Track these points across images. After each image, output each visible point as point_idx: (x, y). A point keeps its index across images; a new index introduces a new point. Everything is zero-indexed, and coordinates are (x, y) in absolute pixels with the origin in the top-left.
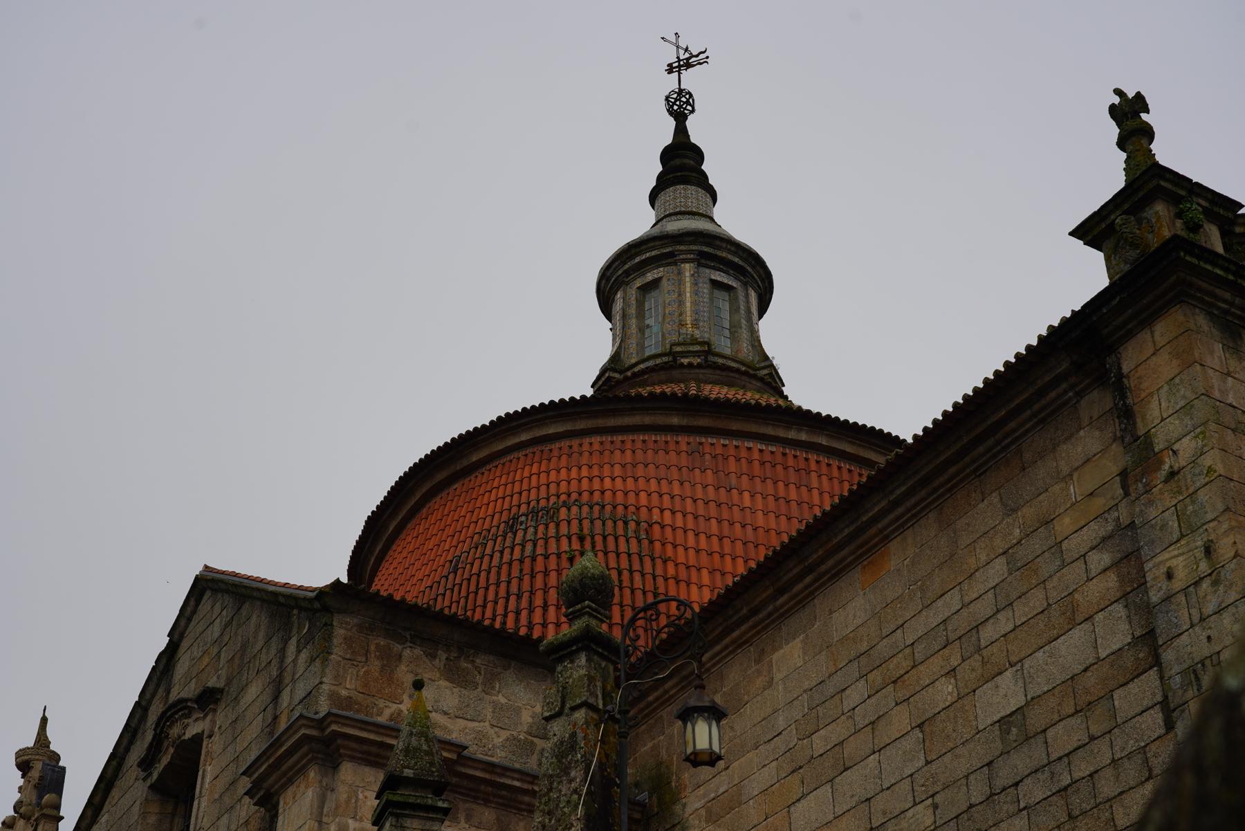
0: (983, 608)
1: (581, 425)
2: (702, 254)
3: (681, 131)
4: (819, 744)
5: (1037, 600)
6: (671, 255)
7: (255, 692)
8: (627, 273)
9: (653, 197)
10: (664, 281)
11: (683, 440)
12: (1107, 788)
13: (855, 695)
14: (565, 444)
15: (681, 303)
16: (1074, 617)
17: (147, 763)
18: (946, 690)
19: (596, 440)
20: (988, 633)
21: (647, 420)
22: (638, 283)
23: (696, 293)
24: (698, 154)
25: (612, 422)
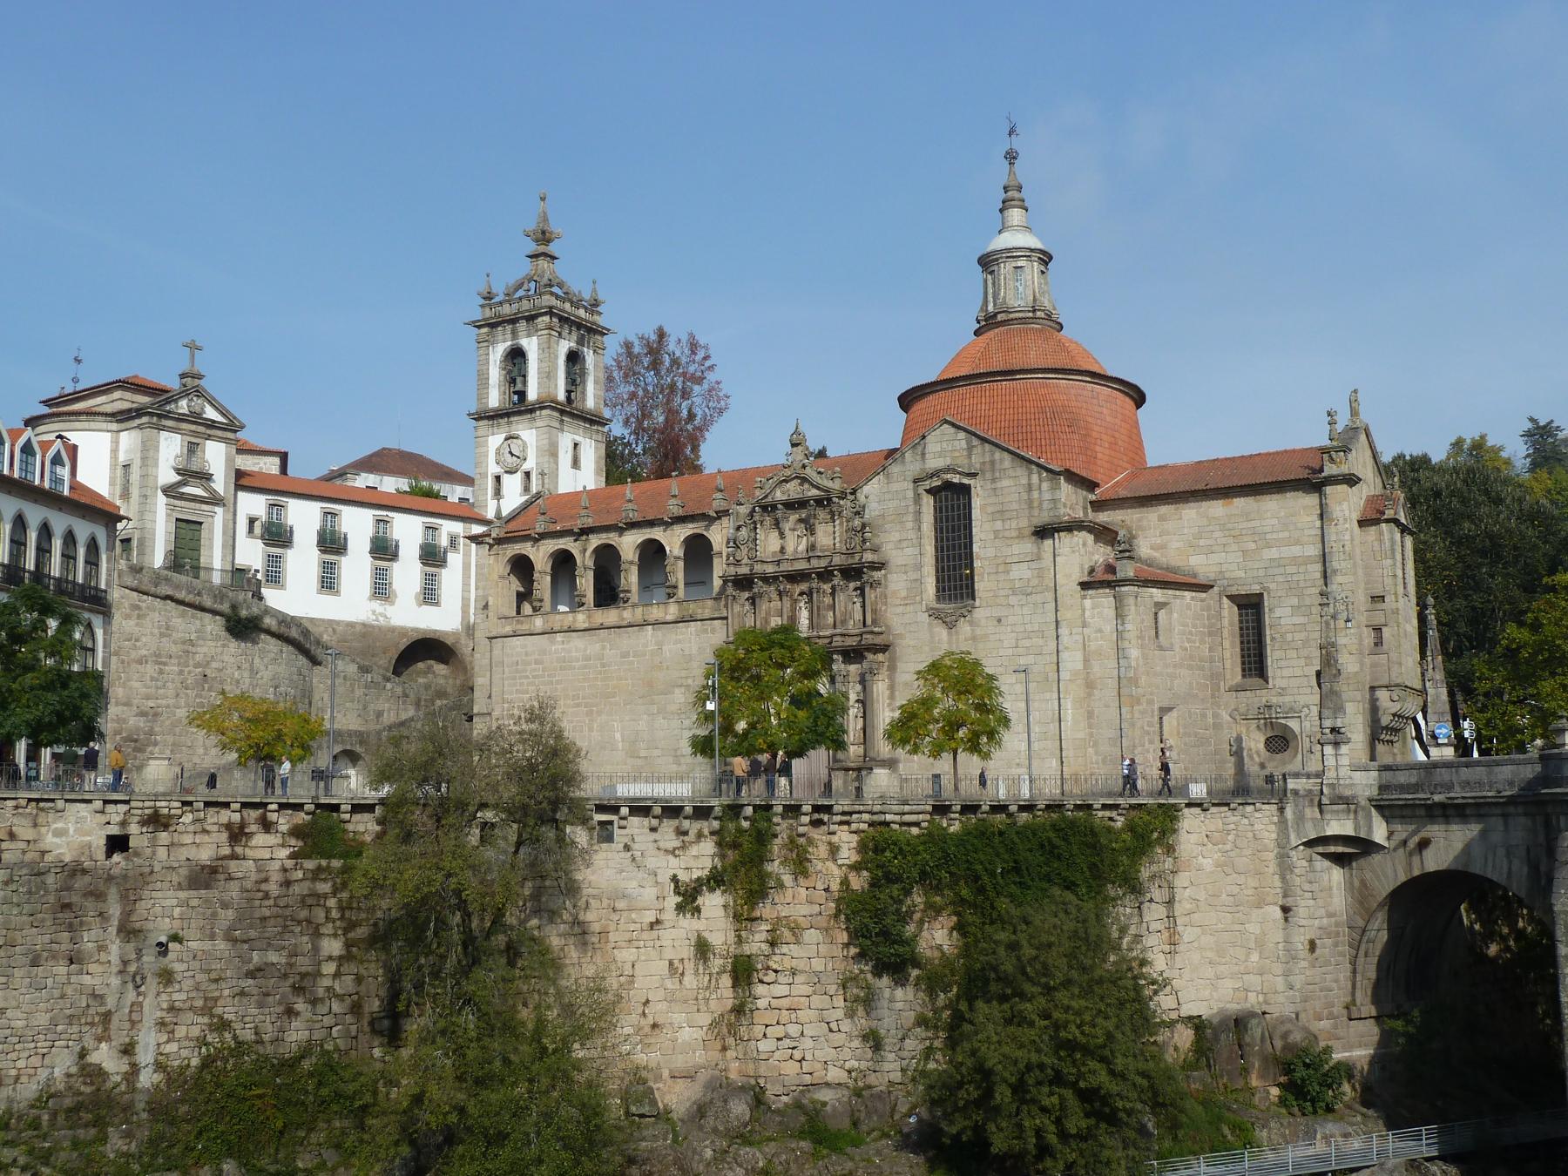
0: (1268, 529)
5: (1286, 534)
7: (1005, 483)
10: (1027, 270)
12: (1302, 584)
16: (1298, 542)
20: (1268, 536)
22: (1014, 264)
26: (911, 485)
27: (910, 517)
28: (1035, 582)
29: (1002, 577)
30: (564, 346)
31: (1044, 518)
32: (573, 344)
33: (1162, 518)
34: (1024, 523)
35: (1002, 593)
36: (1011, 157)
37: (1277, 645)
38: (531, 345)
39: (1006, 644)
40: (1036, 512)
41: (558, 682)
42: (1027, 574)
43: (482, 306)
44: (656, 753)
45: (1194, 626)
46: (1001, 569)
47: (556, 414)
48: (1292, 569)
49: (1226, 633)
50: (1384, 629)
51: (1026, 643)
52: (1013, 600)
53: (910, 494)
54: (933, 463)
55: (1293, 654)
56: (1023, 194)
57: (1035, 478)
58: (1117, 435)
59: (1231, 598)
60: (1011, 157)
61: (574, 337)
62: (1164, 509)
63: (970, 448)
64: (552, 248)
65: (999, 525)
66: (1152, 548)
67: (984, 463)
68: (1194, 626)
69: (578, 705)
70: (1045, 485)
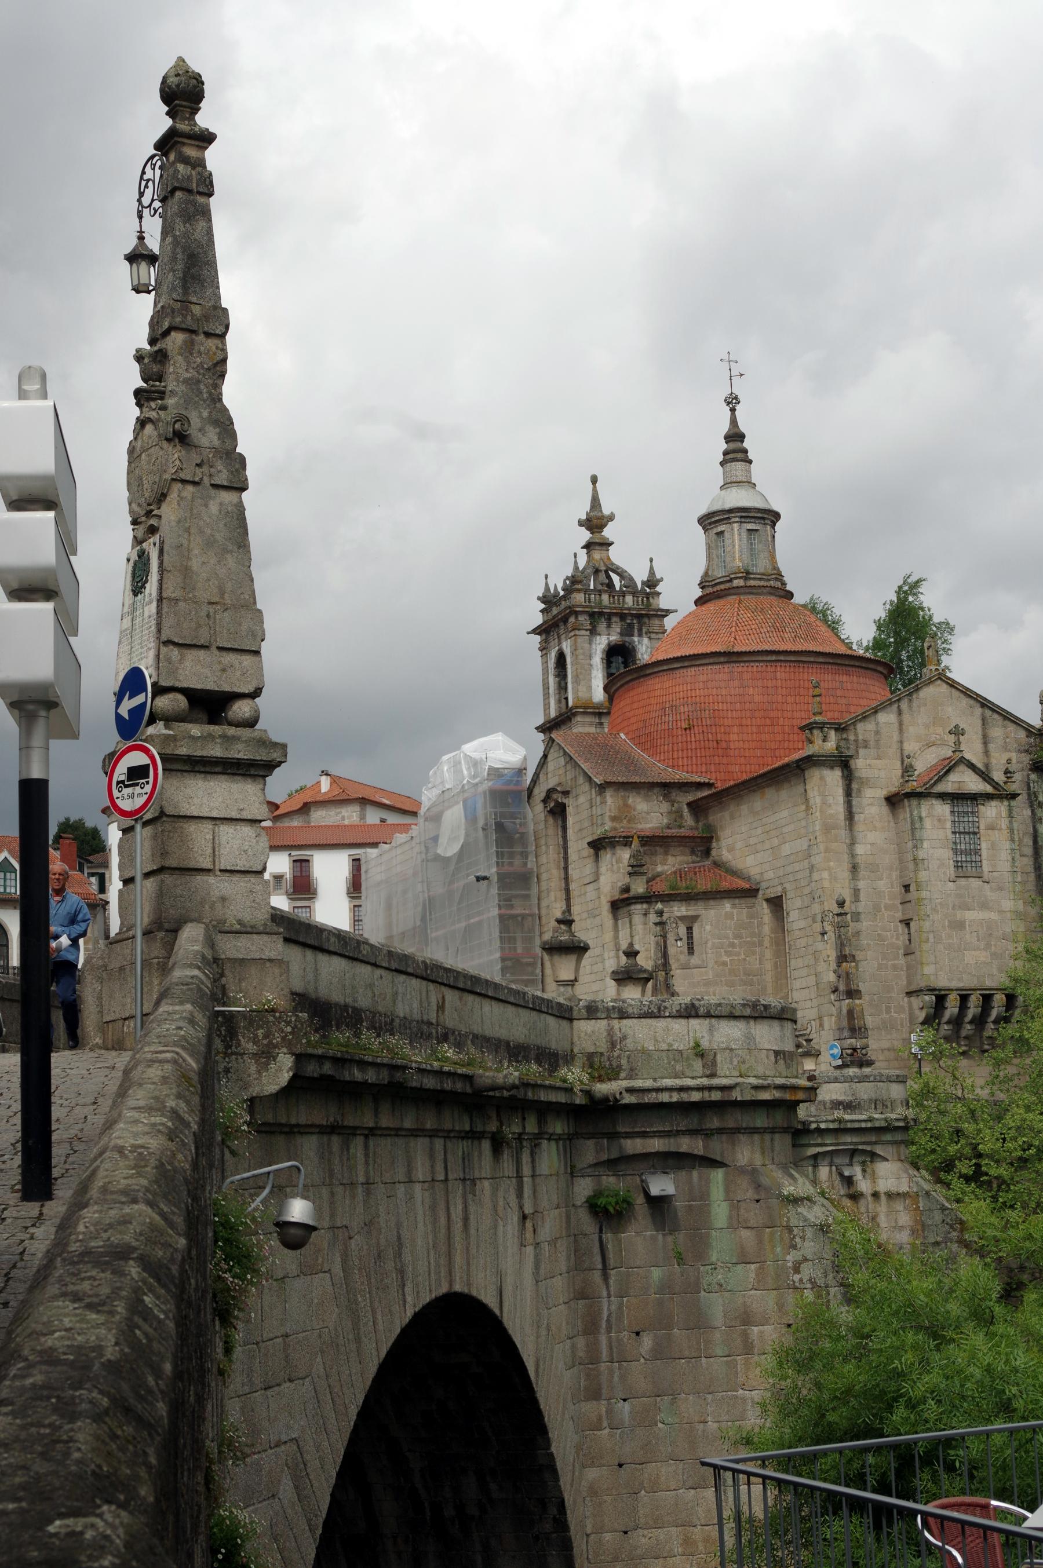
1: (686, 664)
2: (741, 517)
3: (734, 422)
4: (752, 841)
6: (729, 518)
7: (582, 799)
8: (710, 524)
9: (722, 464)
10: (726, 534)
11: (726, 666)
13: (759, 831)
14: (681, 671)
15: (734, 546)
17: (545, 801)
18: (776, 842)
19: (693, 669)
20: (785, 830)
21: (711, 661)
22: (715, 531)
23: (740, 540)
24: (741, 437)
25: (698, 662)
30: (601, 643)
31: (598, 832)
32: (614, 638)
33: (732, 818)
36: (732, 402)
37: (792, 952)
38: (567, 647)
43: (542, 611)
45: (738, 936)
47: (588, 719)
48: (797, 867)
49: (767, 942)
50: (912, 924)
54: (551, 784)
55: (800, 963)
56: (746, 444)
58: (772, 714)
59: (768, 900)
61: (616, 628)
62: (732, 808)
63: (567, 763)
64: (608, 532)
66: (729, 851)
68: (738, 936)
70: (598, 798)
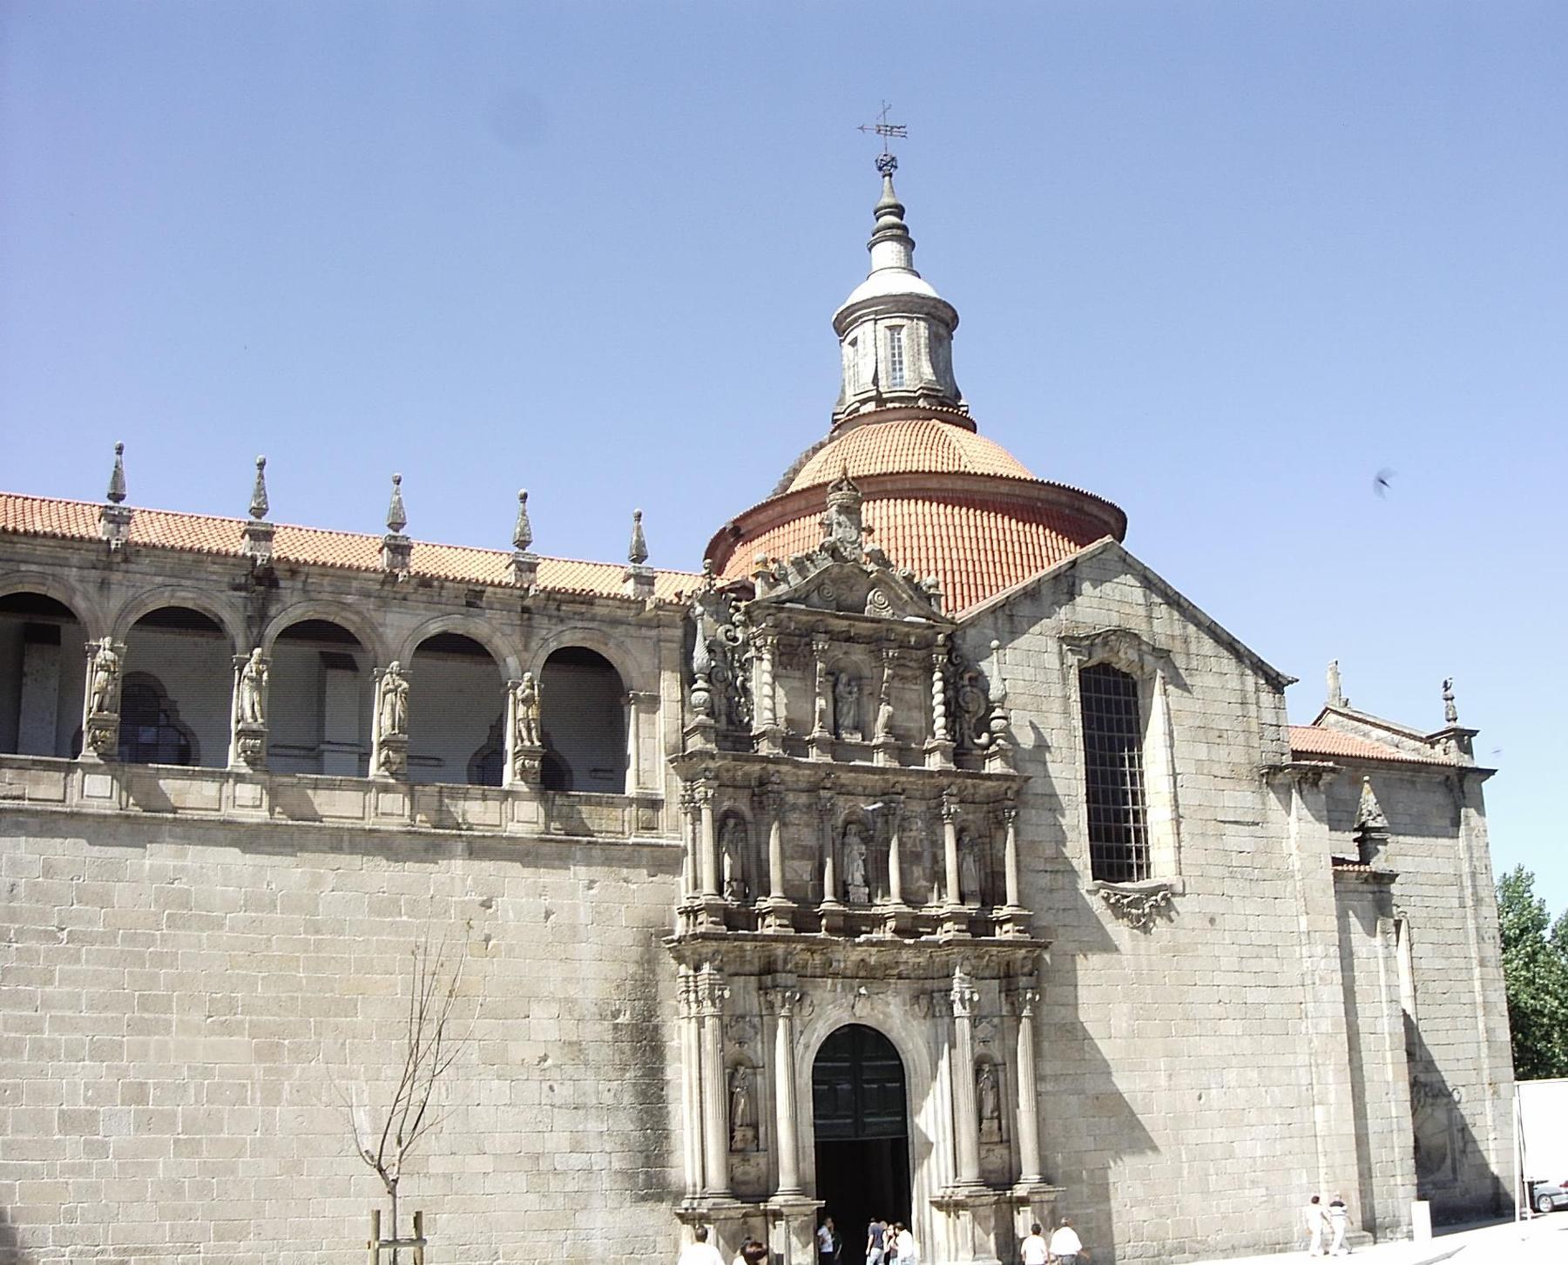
26: (1053, 646)
27: (1057, 706)
28: (1260, 860)
29: (1212, 844)
34: (1239, 755)
35: (1213, 871)
39: (1225, 963)
40: (1255, 742)
41: (160, 960)
42: (1249, 845)
44: (478, 1164)
46: (1212, 828)
51: (1254, 965)
52: (1229, 886)
53: (1052, 661)
57: (1250, 679)
60: (887, 166)
65: (1202, 752)
67: (1173, 637)
69: (228, 1029)
